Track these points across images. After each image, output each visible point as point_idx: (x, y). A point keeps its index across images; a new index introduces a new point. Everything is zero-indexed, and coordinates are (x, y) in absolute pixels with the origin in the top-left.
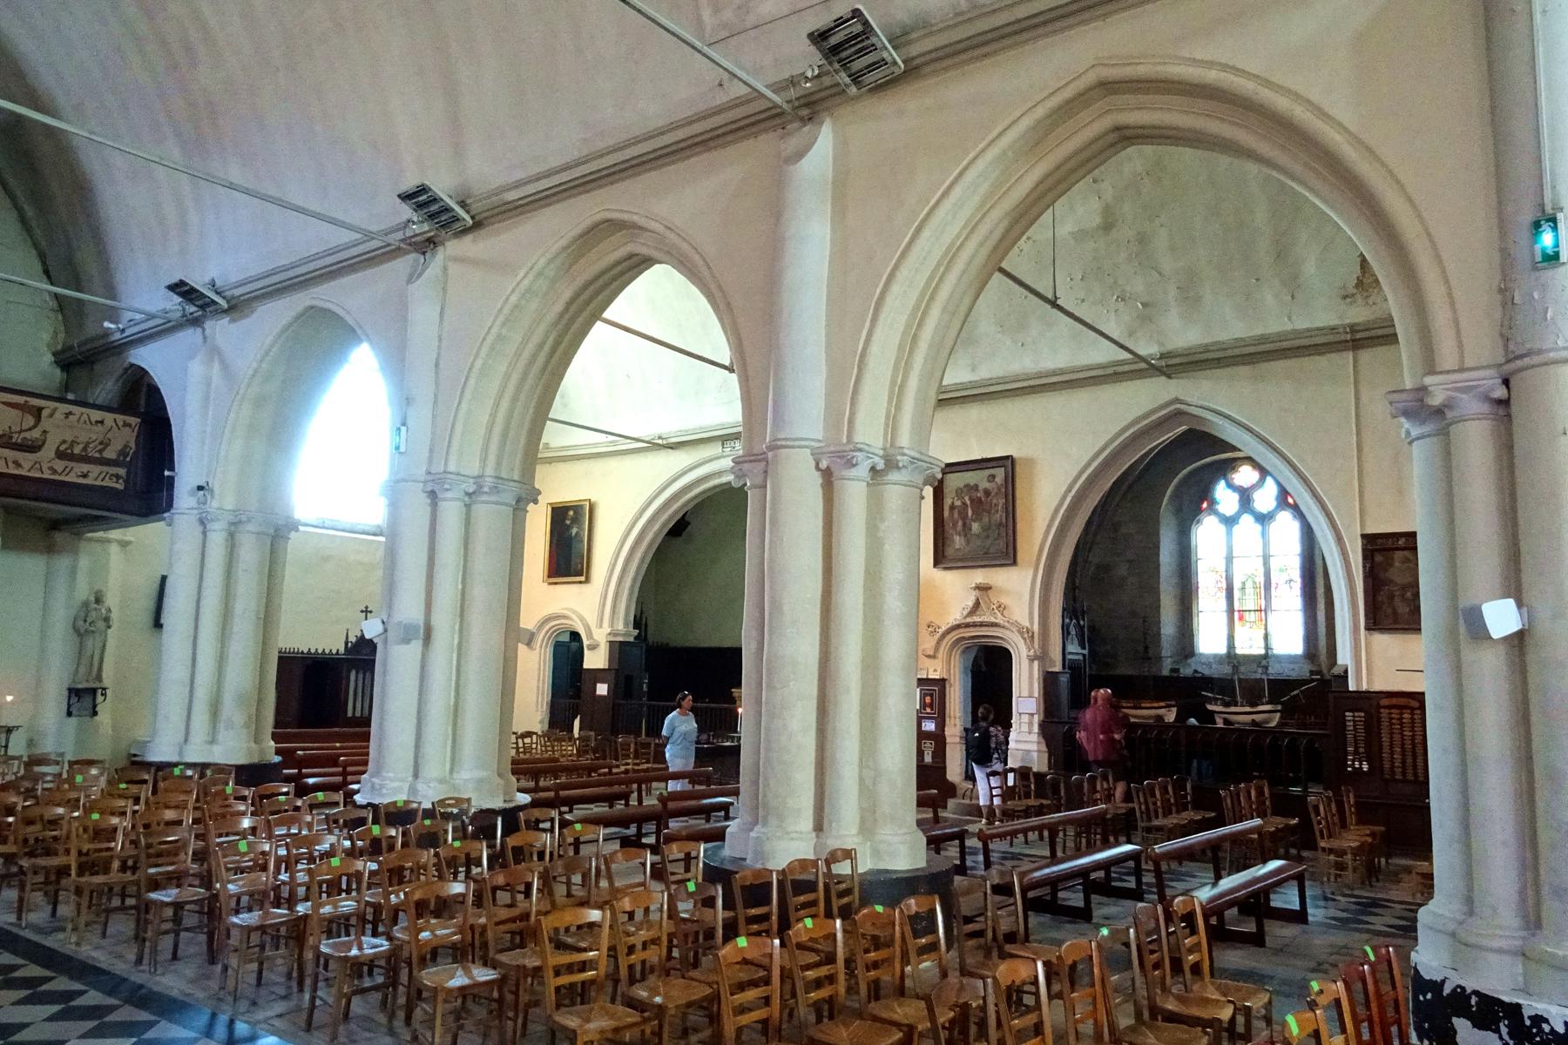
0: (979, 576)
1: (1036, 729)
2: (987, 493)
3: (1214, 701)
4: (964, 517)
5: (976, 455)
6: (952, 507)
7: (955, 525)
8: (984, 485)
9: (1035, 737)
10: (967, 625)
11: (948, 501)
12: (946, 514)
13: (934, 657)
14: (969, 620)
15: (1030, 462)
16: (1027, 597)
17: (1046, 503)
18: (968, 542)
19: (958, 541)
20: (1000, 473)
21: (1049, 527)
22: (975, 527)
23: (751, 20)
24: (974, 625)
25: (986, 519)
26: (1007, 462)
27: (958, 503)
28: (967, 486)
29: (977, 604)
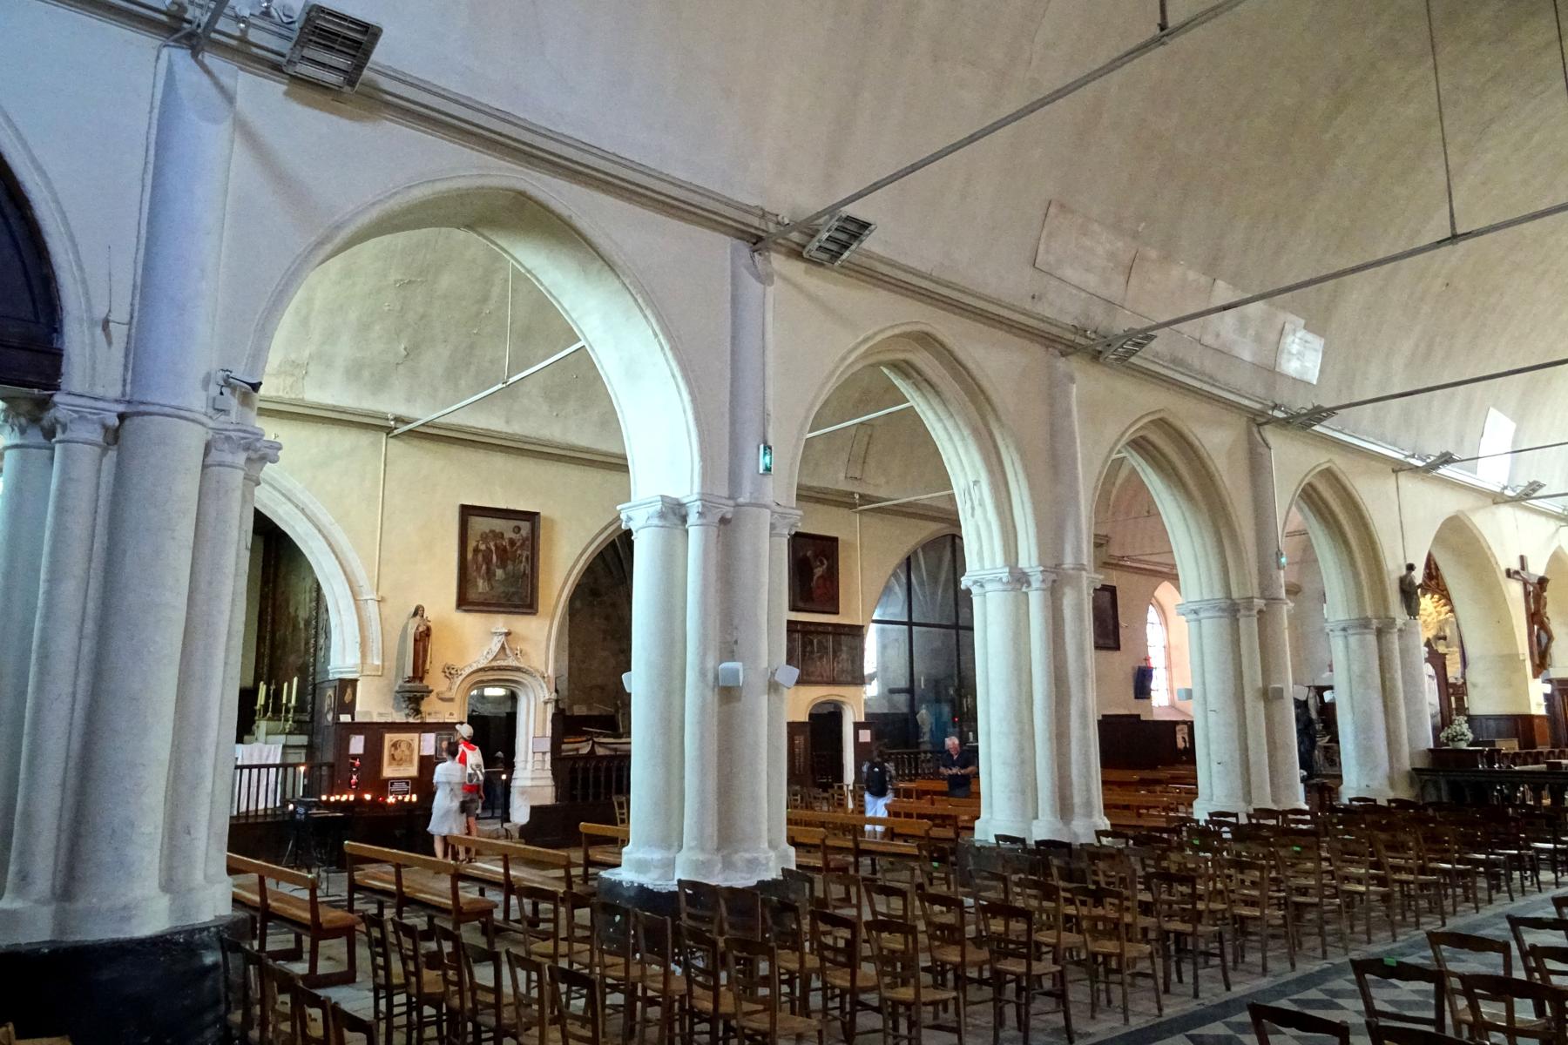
0: (500, 622)
1: (548, 765)
2: (512, 542)
3: (599, 735)
4: (488, 561)
5: (503, 506)
6: (476, 550)
7: (478, 569)
8: (509, 535)
9: (549, 774)
10: (492, 669)
11: (472, 544)
12: (470, 556)
13: (451, 700)
14: (495, 664)
15: (552, 521)
16: (543, 645)
17: (563, 563)
18: (492, 588)
19: (482, 585)
20: (525, 526)
21: (565, 583)
22: (499, 573)
23: (1059, 273)
24: (500, 669)
25: (510, 567)
26: (531, 517)
27: (483, 547)
28: (492, 531)
29: (503, 647)
